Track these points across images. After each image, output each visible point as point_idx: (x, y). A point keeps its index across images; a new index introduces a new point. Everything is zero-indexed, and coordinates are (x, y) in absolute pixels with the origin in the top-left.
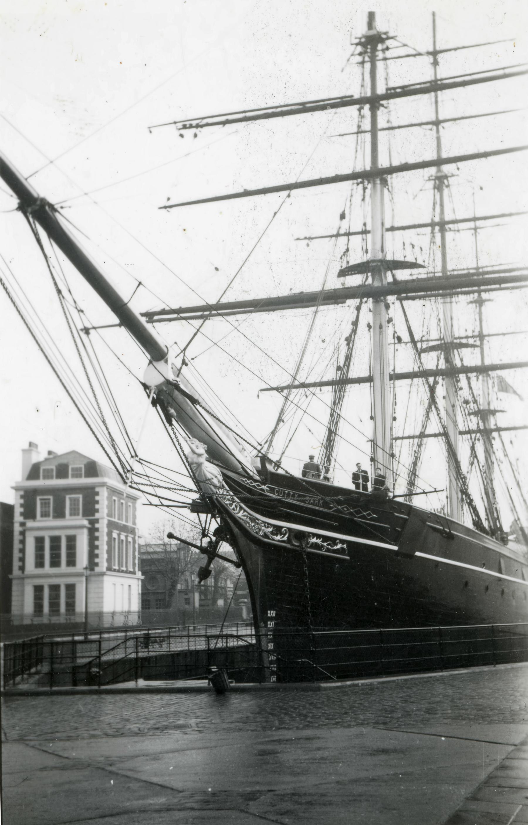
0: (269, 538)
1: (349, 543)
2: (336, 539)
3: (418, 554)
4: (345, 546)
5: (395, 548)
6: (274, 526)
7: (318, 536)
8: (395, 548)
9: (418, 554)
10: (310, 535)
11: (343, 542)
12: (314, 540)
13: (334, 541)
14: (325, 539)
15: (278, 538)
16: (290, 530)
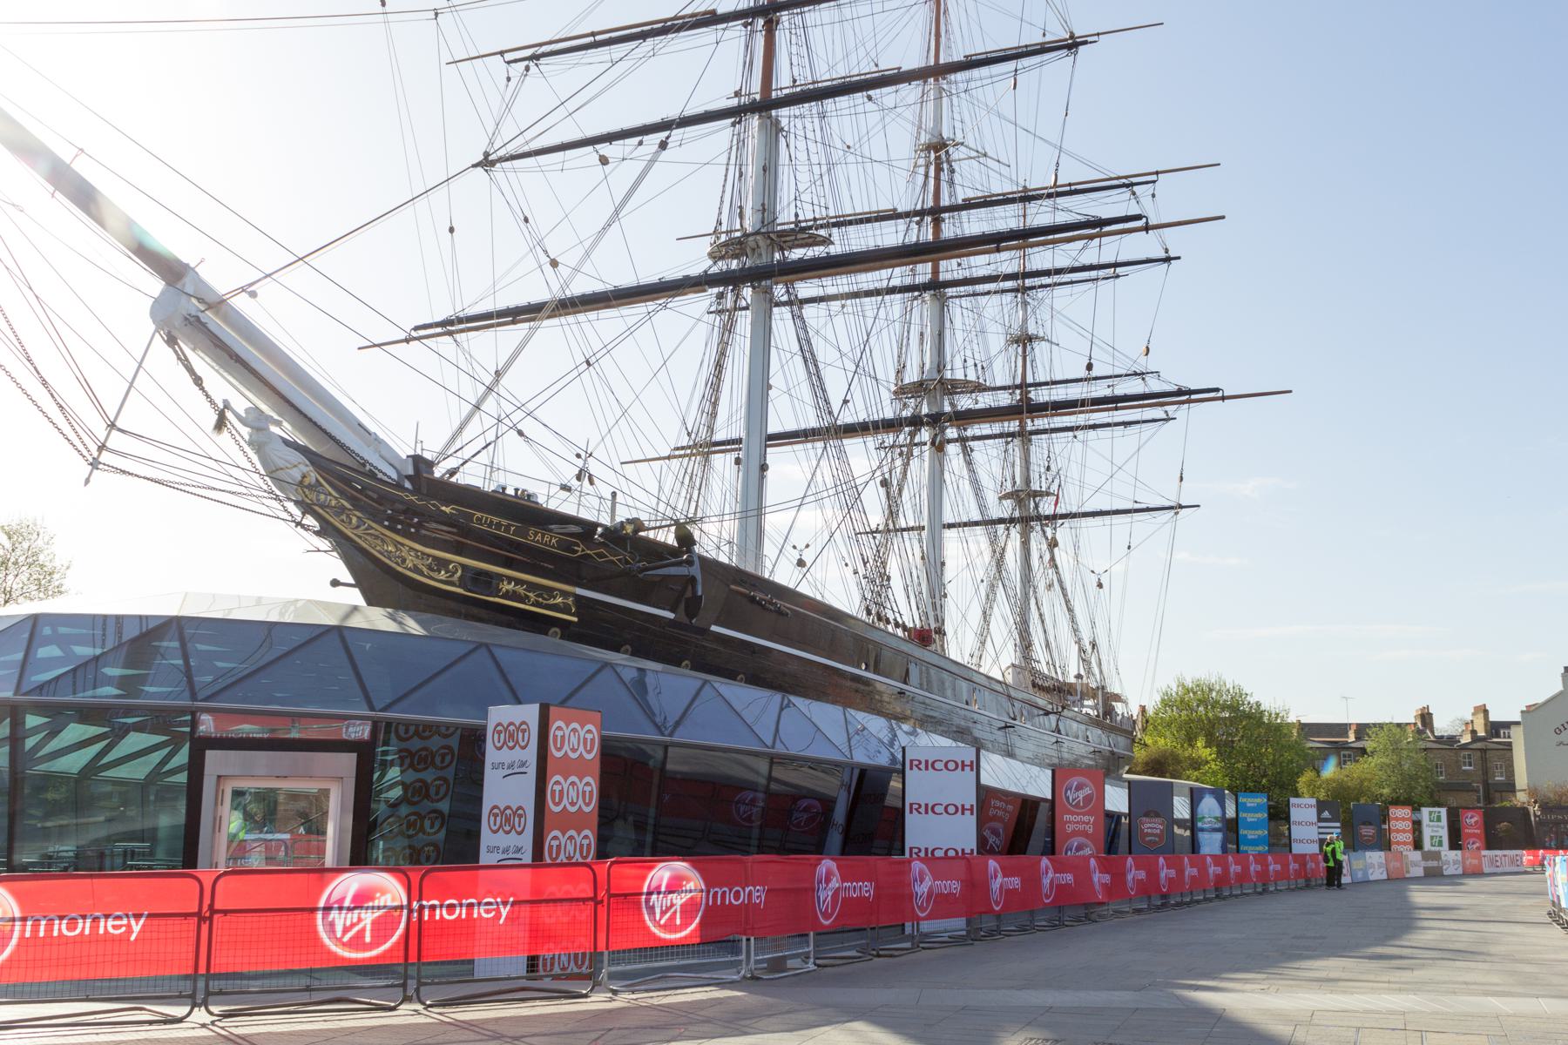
0: (421, 574)
1: (578, 598)
2: (553, 589)
3: (714, 628)
4: (570, 601)
5: (671, 616)
6: (435, 558)
7: (519, 582)
8: (671, 616)
9: (714, 628)
10: (500, 577)
11: (565, 594)
12: (511, 587)
13: (550, 591)
14: (532, 587)
15: (443, 575)
16: (464, 567)
